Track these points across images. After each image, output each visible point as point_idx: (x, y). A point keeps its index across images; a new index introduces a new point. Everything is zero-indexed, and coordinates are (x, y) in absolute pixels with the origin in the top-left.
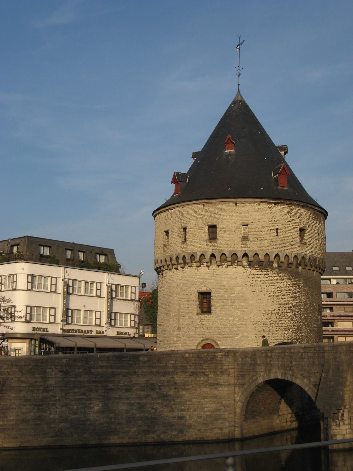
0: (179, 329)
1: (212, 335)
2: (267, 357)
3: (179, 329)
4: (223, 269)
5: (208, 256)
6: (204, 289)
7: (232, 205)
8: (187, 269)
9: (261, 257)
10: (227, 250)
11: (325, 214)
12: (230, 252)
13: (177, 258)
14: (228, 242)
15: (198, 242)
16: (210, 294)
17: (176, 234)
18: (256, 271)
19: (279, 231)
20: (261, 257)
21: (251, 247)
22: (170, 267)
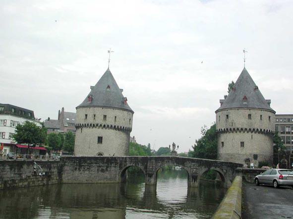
0: (89, 148)
1: (101, 151)
3: (89, 148)
4: (107, 130)
5: (103, 125)
6: (100, 136)
7: (112, 109)
8: (94, 129)
9: (119, 127)
11: (133, 112)
13: (91, 124)
14: (110, 121)
15: (99, 120)
16: (102, 138)
17: (91, 116)
18: (117, 131)
20: (119, 127)
21: (117, 124)
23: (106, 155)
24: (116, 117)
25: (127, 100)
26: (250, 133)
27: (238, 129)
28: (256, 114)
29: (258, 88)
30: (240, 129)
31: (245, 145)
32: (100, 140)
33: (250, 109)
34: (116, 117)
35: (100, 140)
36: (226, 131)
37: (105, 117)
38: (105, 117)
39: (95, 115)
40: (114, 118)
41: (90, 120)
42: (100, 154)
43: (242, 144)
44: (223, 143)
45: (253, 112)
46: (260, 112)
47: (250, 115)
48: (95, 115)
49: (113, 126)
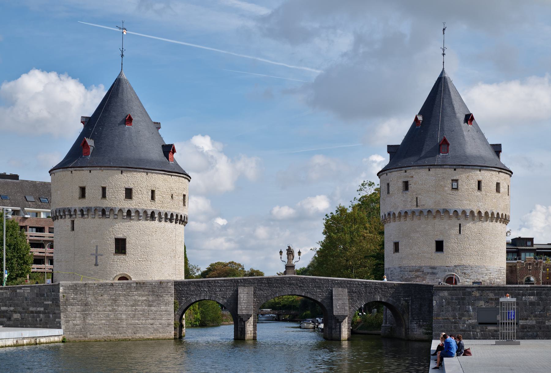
0: (96, 265)
2: (199, 286)
6: (120, 236)
12: (143, 209)
14: (141, 201)
19: (174, 196)
22: (86, 216)
24: (153, 192)
26: (454, 220)
29: (472, 118)
30: (434, 212)
31: (445, 248)
32: (121, 246)
33: (456, 167)
34: (153, 192)
37: (129, 193)
38: (129, 193)
39: (104, 189)
40: (150, 193)
41: (93, 200)
43: (440, 246)
44: (396, 245)
49: (149, 213)
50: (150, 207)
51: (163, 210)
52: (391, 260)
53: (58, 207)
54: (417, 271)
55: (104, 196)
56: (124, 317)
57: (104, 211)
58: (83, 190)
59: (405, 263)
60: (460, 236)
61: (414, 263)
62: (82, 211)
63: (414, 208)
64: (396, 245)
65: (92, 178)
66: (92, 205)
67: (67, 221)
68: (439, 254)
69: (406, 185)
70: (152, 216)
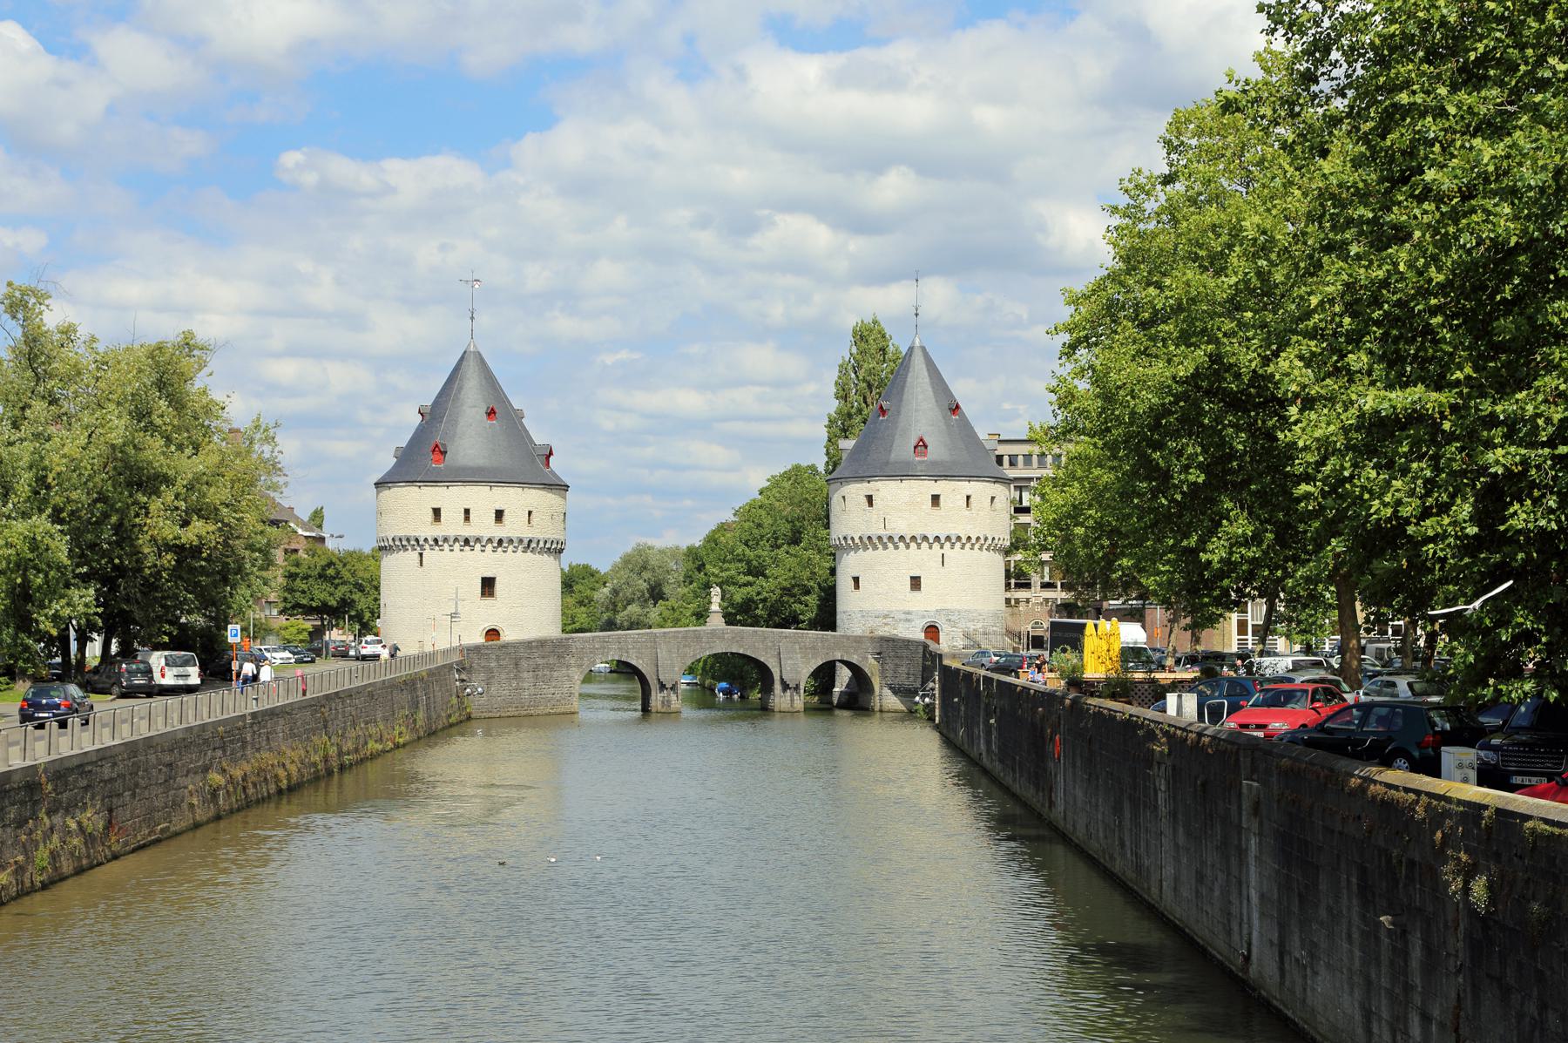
10: (514, 535)
14: (514, 526)
15: (483, 525)
23: (508, 636)
25: (551, 453)
26: (936, 546)
27: (902, 538)
28: (953, 491)
29: (958, 407)
32: (488, 585)
33: (937, 477)
35: (488, 585)
36: (869, 542)
37: (499, 515)
38: (499, 515)
39: (467, 511)
41: (452, 525)
42: (493, 633)
43: (916, 583)
44: (856, 580)
45: (941, 487)
46: (967, 487)
47: (936, 499)
48: (467, 511)
50: (527, 534)
51: (540, 536)
52: (848, 601)
53: (401, 533)
54: (886, 616)
55: (467, 518)
56: (526, 685)
57: (467, 542)
58: (437, 512)
59: (867, 606)
60: (942, 570)
61: (881, 606)
62: (436, 541)
63: (881, 532)
64: (856, 580)
65: (452, 498)
66: (452, 533)
67: (413, 556)
68: (916, 593)
69: (870, 499)
70: (528, 545)
